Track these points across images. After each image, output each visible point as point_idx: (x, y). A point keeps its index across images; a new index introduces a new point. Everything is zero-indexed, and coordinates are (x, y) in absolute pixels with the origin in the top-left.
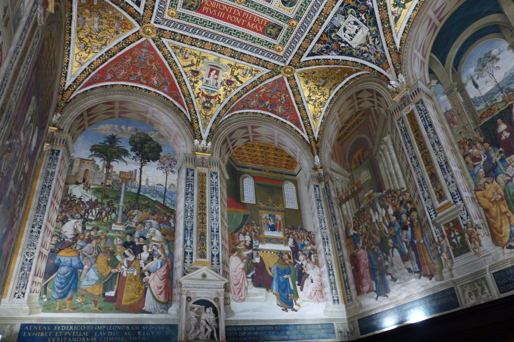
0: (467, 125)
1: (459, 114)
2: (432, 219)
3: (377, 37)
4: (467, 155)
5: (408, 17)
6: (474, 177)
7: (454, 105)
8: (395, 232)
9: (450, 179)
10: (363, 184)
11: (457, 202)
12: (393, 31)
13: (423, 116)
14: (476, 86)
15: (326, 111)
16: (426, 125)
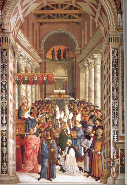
2: (113, 141)
8: (77, 136)
10: (57, 80)
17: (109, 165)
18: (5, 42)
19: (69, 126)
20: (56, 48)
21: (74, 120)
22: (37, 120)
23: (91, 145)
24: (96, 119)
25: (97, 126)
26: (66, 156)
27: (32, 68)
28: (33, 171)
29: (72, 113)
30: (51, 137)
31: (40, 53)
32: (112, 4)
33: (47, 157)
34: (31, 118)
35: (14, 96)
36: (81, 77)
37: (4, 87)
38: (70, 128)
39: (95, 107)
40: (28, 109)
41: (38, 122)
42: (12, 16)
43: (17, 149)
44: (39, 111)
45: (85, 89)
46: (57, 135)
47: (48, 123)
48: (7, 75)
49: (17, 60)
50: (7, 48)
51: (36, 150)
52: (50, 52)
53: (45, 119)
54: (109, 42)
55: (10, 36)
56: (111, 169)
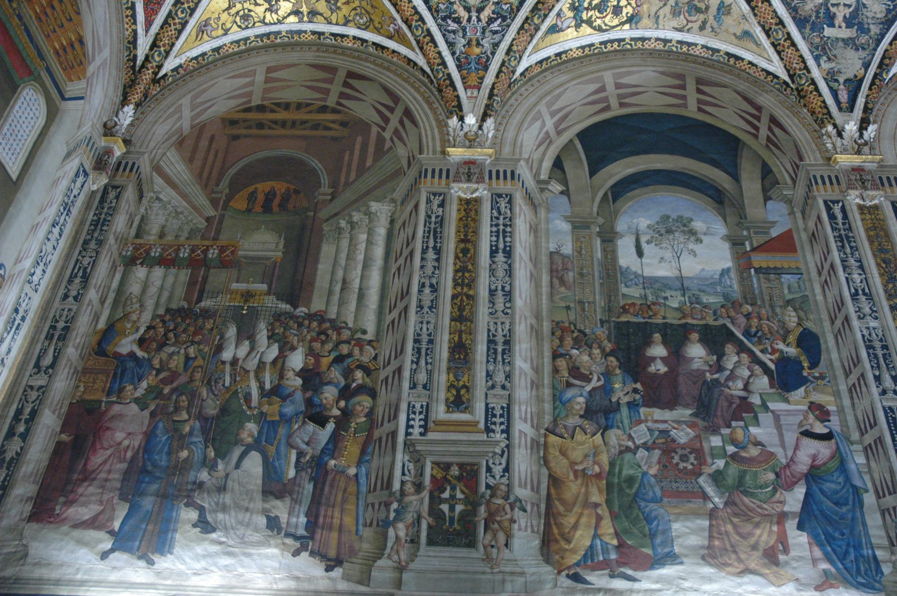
0: (589, 303)
1: (581, 275)
2: (408, 434)
3: (504, 19)
4: (562, 355)
5: (566, 47)
6: (558, 403)
7: (580, 252)
8: (281, 415)
9: (500, 378)
10: (246, 257)
11: (493, 431)
12: (534, 41)
13: (497, 225)
14: (640, 253)
15: (237, 42)
16: (496, 246)
17: (383, 515)
18: (124, 170)
19: (260, 383)
20: (263, 187)
21: (279, 365)
22: (156, 363)
23: (327, 444)
24: (352, 367)
25: (354, 385)
26: (227, 475)
27: (180, 229)
28: (92, 523)
29: (277, 344)
30: (188, 413)
31: (214, 195)
32: (436, 105)
33: (159, 478)
34: (140, 353)
35: (104, 295)
36: (322, 255)
37: (81, 271)
38: (261, 387)
39: (353, 331)
40: (137, 330)
41: (158, 366)
42: (161, 120)
43: (59, 448)
44: (171, 335)
45: (331, 284)
46: (211, 408)
47: (191, 370)
48: (100, 243)
49: (142, 210)
50: (122, 183)
51: (126, 451)
52: (244, 193)
53: (182, 359)
54: (420, 177)
55: (141, 159)
56: (391, 532)
